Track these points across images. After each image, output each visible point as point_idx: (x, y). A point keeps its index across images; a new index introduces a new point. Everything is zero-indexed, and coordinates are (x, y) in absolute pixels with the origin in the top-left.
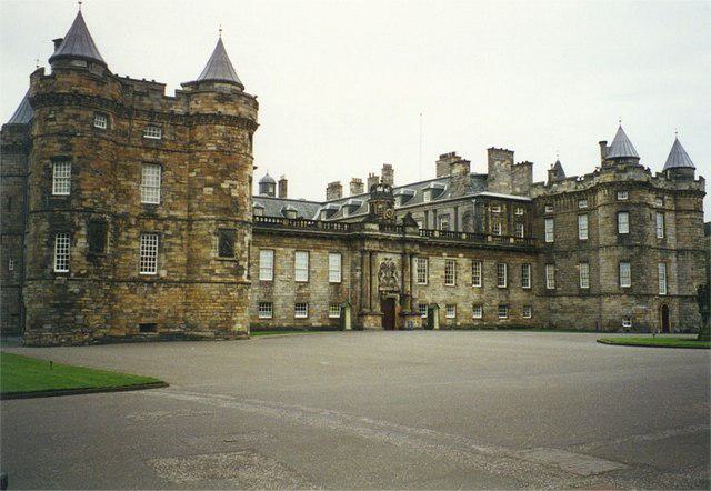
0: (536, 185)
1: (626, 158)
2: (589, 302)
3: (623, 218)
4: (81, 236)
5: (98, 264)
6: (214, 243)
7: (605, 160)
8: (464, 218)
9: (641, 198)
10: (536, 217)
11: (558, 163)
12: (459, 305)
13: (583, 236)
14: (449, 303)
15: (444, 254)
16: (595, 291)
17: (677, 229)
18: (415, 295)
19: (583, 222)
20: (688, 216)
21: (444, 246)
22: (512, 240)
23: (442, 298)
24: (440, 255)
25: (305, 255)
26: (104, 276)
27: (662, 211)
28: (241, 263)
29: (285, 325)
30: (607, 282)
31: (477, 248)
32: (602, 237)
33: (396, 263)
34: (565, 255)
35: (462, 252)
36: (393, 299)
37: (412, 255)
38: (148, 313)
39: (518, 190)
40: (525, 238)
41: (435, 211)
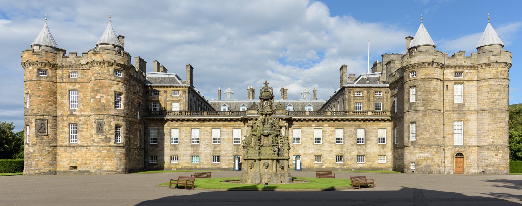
4: (33, 127)
5: (42, 139)
6: (94, 126)
9: (426, 74)
14: (316, 154)
15: (313, 125)
20: (487, 83)
21: (310, 120)
22: (369, 113)
23: (311, 151)
24: (310, 126)
25: (219, 130)
26: (46, 144)
27: (457, 82)
28: (108, 136)
29: (206, 167)
35: (326, 124)
38: (73, 161)
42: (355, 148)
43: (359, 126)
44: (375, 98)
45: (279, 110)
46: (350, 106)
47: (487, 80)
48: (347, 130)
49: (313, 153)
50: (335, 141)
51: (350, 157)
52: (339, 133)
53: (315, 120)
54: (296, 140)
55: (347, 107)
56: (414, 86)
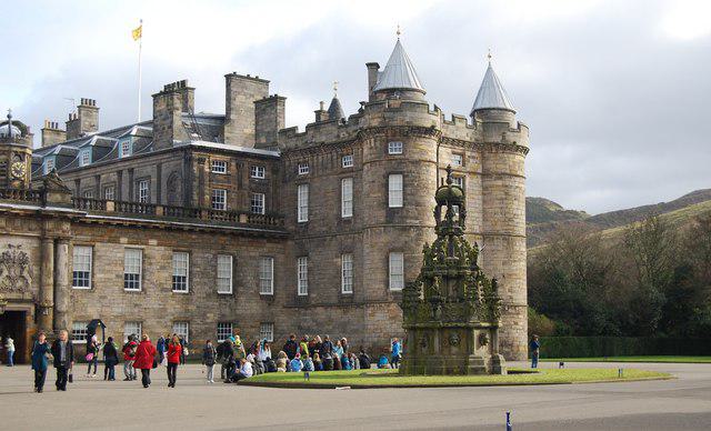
0: (285, 132)
1: (402, 90)
2: (353, 315)
3: (396, 183)
7: (374, 94)
8: (170, 182)
10: (285, 182)
11: (335, 103)
12: (149, 322)
13: (347, 213)
15: (124, 240)
16: (358, 298)
17: (484, 202)
18: (64, 304)
19: (347, 188)
20: (500, 183)
22: (243, 219)
23: (117, 310)
24: (115, 241)
30: (374, 287)
31: (180, 230)
32: (366, 214)
33: (29, 254)
34: (321, 239)
36: (21, 315)
37: (57, 241)
39: (263, 140)
40: (268, 216)
41: (131, 171)
42: (214, 303)
43: (223, 248)
44: (252, 181)
45: (55, 191)
46: (201, 195)
47: (501, 176)
48: (199, 256)
49: (121, 316)
50: (169, 284)
51: (203, 327)
52: (181, 265)
53: (133, 226)
54: (80, 278)
55: (196, 197)
56: (401, 173)
